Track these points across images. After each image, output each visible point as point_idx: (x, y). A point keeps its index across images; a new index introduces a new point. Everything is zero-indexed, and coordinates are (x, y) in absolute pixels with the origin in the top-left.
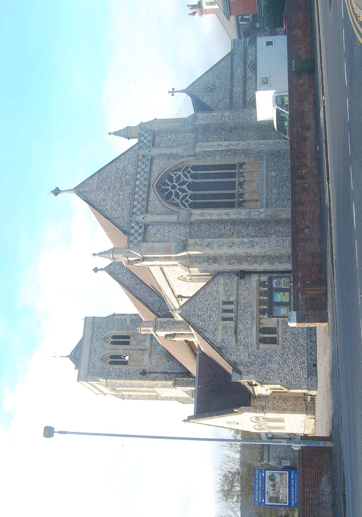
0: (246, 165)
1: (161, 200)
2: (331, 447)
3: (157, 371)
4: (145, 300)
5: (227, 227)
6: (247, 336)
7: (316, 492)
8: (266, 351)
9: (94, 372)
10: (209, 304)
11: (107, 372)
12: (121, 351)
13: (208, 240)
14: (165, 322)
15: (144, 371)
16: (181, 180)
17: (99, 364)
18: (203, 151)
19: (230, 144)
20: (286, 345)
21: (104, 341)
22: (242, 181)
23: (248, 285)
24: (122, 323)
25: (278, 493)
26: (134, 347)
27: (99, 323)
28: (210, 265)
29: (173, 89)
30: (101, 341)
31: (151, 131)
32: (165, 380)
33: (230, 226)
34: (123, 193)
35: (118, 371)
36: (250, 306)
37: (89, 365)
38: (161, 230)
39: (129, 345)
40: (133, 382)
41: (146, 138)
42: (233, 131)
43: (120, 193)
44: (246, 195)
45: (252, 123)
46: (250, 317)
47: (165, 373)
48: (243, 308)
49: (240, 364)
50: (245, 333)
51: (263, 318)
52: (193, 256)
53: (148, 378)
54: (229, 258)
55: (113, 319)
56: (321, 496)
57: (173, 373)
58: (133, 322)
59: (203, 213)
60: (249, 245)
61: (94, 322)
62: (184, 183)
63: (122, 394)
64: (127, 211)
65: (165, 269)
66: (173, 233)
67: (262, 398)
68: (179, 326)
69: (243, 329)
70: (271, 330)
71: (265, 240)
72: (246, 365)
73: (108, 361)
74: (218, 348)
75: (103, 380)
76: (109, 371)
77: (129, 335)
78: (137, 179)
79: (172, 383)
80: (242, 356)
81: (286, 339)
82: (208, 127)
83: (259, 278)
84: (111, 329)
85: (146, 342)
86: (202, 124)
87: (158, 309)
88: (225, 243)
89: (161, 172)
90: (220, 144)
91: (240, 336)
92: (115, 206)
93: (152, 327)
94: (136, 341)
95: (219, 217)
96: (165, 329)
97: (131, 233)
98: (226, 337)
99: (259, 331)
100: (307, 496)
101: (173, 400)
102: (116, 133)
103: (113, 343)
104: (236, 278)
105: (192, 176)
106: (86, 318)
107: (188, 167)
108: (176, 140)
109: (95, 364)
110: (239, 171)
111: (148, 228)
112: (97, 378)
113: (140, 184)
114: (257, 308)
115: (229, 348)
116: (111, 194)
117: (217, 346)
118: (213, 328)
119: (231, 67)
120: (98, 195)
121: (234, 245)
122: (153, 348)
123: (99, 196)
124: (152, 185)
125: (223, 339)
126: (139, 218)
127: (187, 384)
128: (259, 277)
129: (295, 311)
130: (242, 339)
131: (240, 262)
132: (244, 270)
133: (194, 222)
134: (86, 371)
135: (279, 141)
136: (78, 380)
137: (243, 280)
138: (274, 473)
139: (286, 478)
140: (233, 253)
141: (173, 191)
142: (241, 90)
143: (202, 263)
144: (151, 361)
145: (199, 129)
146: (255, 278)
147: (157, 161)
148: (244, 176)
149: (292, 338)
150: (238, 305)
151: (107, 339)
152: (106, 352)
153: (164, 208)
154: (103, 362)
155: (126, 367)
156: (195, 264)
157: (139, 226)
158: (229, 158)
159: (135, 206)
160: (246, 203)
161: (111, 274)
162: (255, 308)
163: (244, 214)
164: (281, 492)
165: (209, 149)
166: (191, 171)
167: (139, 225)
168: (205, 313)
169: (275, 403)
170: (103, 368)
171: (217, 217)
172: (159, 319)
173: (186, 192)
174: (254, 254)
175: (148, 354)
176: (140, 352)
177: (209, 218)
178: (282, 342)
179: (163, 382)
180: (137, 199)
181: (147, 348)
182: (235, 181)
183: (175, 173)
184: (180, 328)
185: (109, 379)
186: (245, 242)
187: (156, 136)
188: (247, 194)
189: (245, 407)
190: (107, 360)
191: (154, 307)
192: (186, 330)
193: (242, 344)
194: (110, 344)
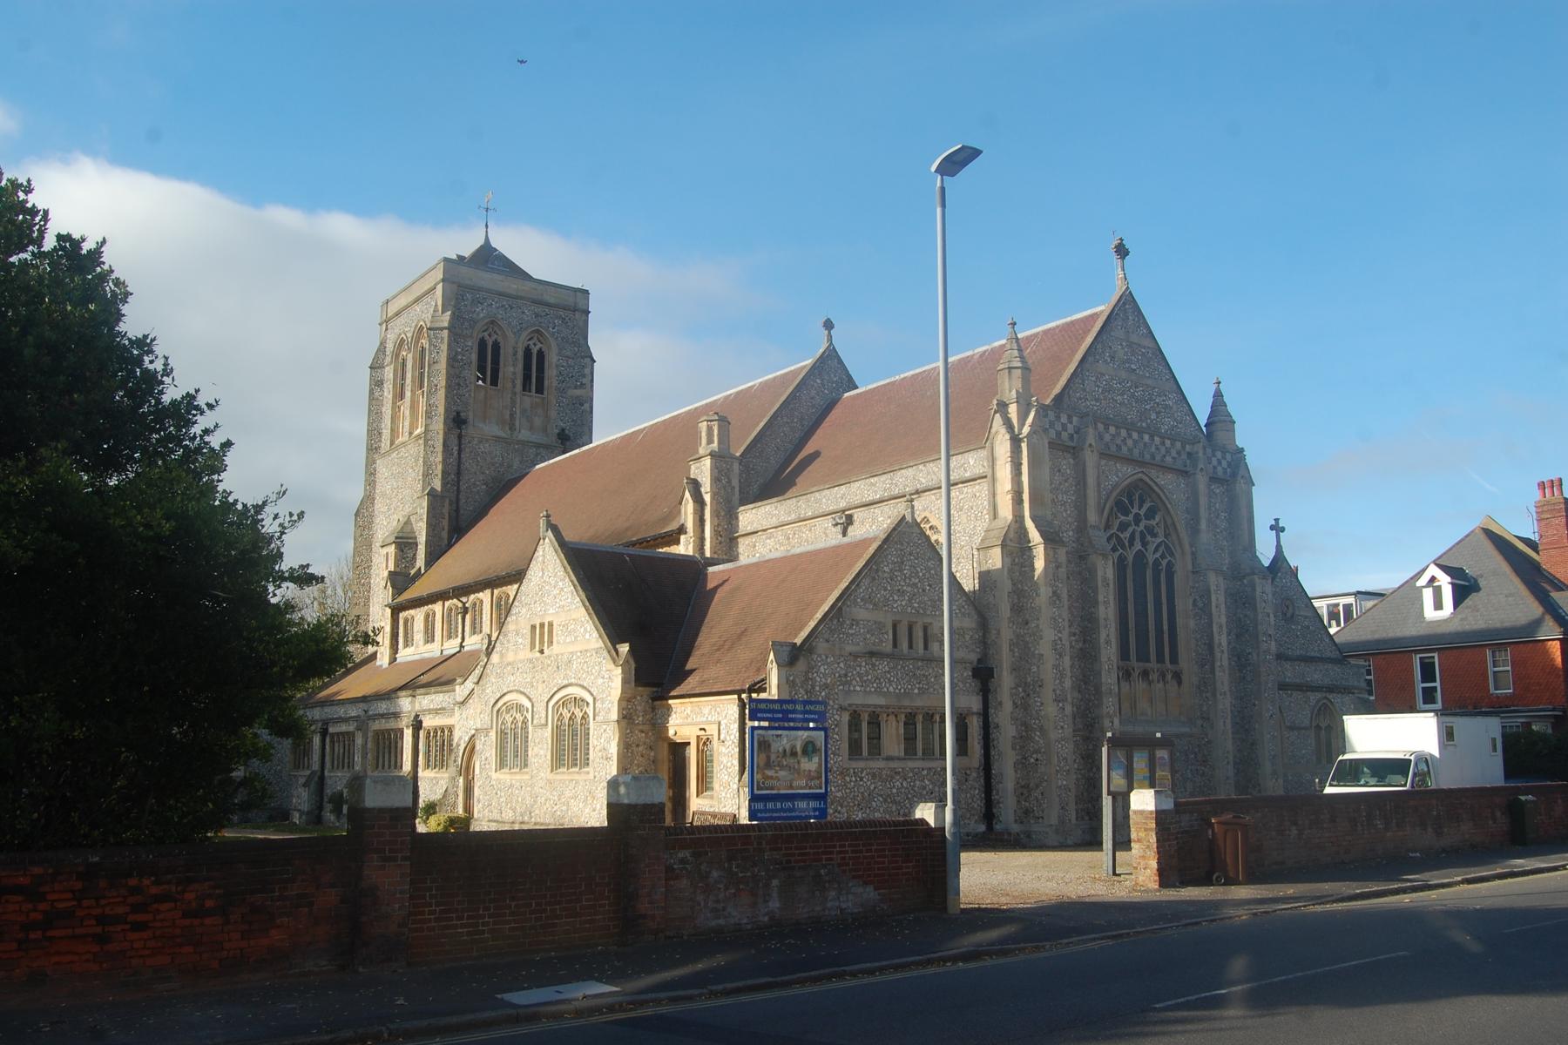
1: (1118, 491)
2: (945, 909)
4: (771, 435)
5: (1076, 641)
6: (865, 682)
7: (844, 871)
8: (837, 730)
10: (924, 591)
11: (464, 334)
12: (512, 369)
13: (1065, 595)
14: (729, 482)
15: (464, 422)
16: (1149, 538)
17: (482, 315)
18: (1209, 591)
19: (1223, 651)
20: (848, 779)
23: (961, 686)
24: (572, 376)
25: (779, 765)
26: (518, 401)
28: (1008, 596)
29: (1283, 529)
31: (1234, 475)
32: (443, 472)
33: (1078, 647)
34: (1126, 401)
36: (922, 692)
37: (480, 289)
38: (1066, 484)
40: (442, 393)
41: (1219, 462)
42: (1235, 659)
43: (1126, 397)
44: (1128, 683)
45: (1257, 703)
46: (902, 690)
47: (459, 473)
48: (918, 672)
49: (809, 663)
50: (870, 677)
51: (898, 722)
52: (1025, 557)
53: (449, 430)
54: (1021, 643)
55: (583, 357)
56: (836, 886)
57: (458, 491)
60: (1058, 692)
61: (577, 310)
62: (1144, 544)
63: (387, 365)
64: (1095, 408)
65: (982, 489)
66: (1062, 513)
67: (651, 716)
68: (723, 514)
69: (879, 671)
70: (875, 741)
71: (1069, 731)
72: (807, 679)
73: (487, 338)
74: (840, 608)
75: (445, 320)
77: (545, 392)
78: (1152, 437)
80: (825, 670)
81: (861, 780)
82: (1244, 604)
83: (973, 714)
86: (1254, 590)
87: (751, 466)
88: (1060, 635)
91: (864, 664)
92: (1104, 383)
93: (719, 448)
94: (531, 407)
95: (1102, 622)
96: (715, 480)
97: (1062, 415)
98: (862, 631)
99: (874, 712)
100: (834, 846)
101: (366, 490)
102: (1218, 395)
103: (528, 352)
104: (973, 657)
105: (1157, 563)
106: (587, 292)
107: (1172, 554)
108: (1218, 531)
111: (1069, 455)
113: (1145, 444)
114: (918, 708)
115: (841, 636)
116: (1123, 374)
117: (843, 609)
118: (879, 599)
119: (1323, 658)
120: (1121, 345)
121: (1058, 657)
123: (1119, 347)
124: (1144, 470)
125: (857, 624)
126: (1091, 439)
127: (435, 526)
128: (978, 714)
129: (1175, 805)
130: (858, 669)
131: (1014, 669)
132: (993, 677)
133: (1086, 564)
134: (468, 282)
135: (1232, 763)
136: (446, 260)
137: (970, 673)
138: (821, 755)
139: (810, 788)
140: (1037, 652)
141: (1131, 517)
142: (1287, 680)
143: (1012, 581)
144: (487, 440)
145: (1239, 583)
146: (975, 703)
149: (862, 793)
150: (925, 662)
151: (538, 339)
154: (487, 324)
156: (1008, 560)
157: (1073, 435)
159: (1107, 428)
161: (823, 359)
162: (918, 703)
163: (1109, 681)
164: (782, 773)
165: (1213, 604)
166: (1166, 561)
167: (1075, 435)
168: (908, 581)
169: (641, 749)
172: (736, 466)
173: (1130, 548)
174: (1036, 701)
175: (504, 435)
176: (507, 417)
177: (1101, 598)
178: (854, 769)
179: (440, 467)
180: (1118, 434)
182: (1148, 661)
184: (718, 517)
185: (449, 336)
186: (1064, 682)
187: (1223, 485)
188: (1128, 687)
189: (633, 672)
190: (490, 335)
191: (755, 456)
192: (715, 531)
193: (849, 670)
194: (525, 345)
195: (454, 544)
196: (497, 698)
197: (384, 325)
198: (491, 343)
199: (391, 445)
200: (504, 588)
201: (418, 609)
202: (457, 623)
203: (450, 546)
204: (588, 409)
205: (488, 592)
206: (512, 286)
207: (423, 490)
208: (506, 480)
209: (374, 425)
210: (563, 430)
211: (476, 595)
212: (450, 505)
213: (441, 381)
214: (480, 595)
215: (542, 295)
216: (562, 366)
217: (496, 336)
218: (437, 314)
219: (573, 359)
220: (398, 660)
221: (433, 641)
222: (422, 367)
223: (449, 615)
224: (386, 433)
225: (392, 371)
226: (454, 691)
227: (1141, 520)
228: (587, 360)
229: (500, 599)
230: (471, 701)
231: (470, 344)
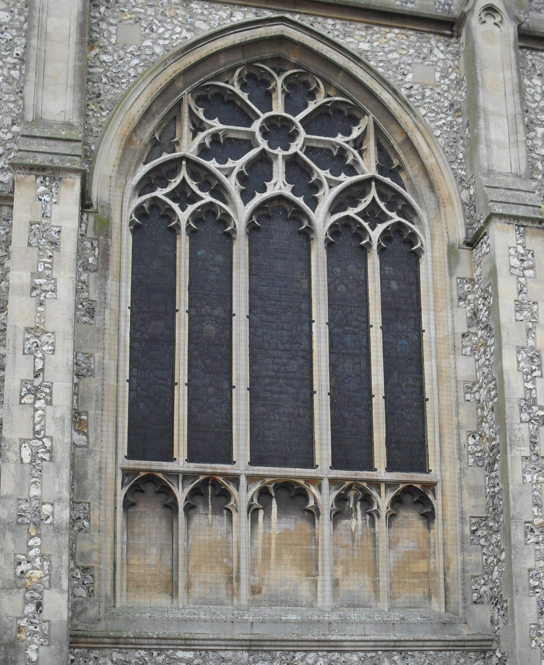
0: (425, 530)
16: (323, 174)
22: (312, 503)
59: (53, 243)
89: (368, 68)
90: (539, 366)
110: (376, 484)
141: (256, 127)
147: (442, 56)
148: (349, 517)
153: (135, 67)
158: (459, 427)
160: (164, 524)
163: (35, 491)
171: (22, 324)
173: (246, 196)
183: (371, 145)
227: (296, 133)
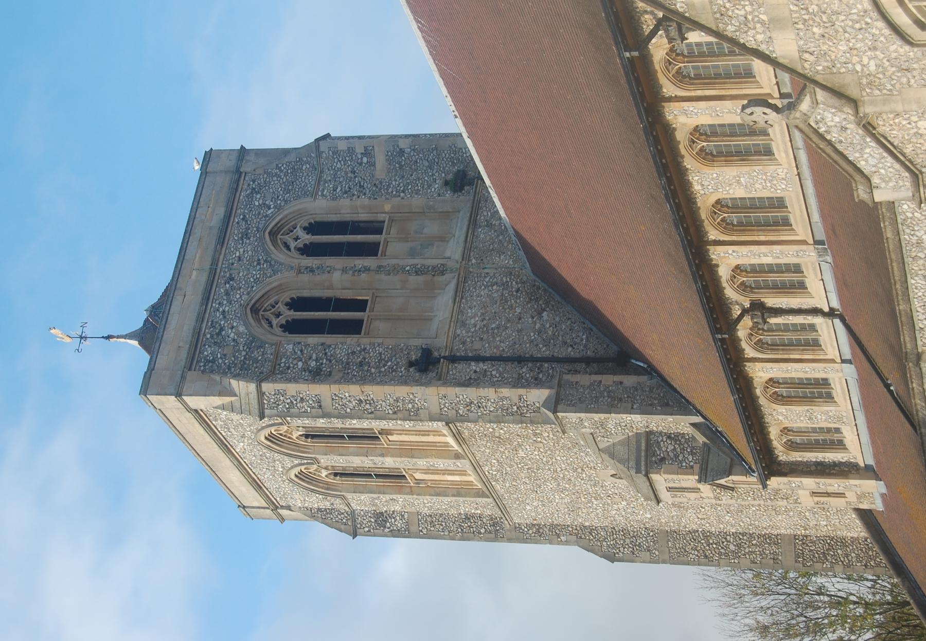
3: (483, 354)
9: (213, 361)
12: (337, 275)
17: (242, 329)
21: (274, 242)
24: (353, 172)
26: (393, 262)
27: (257, 172)
30: (262, 239)
32: (515, 386)
35: (314, 357)
37: (197, 333)
39: (377, 256)
40: (375, 392)
47: (520, 360)
53: (440, 379)
55: (319, 154)
57: (552, 360)
58: (401, 167)
63: (348, 505)
73: (282, 320)
75: (244, 388)
76: (277, 355)
77: (381, 217)
79: (543, 398)
84: (305, 194)
85: (451, 243)
94: (406, 240)
101: (567, 543)
103: (308, 250)
109: (222, 329)
112: (225, 381)
122: (474, 261)
127: (613, 399)
134: (184, 355)
152: (275, 281)
154: (258, 321)
155: (351, 340)
170: (253, 343)
175: (452, 285)
176: (420, 279)
179: (505, 392)
181: (450, 264)
185: (275, 381)
190: (278, 315)
195: (645, 360)
196: (887, 31)
197: (281, 511)
198: (292, 313)
199: (483, 495)
200: (703, 216)
201: (768, 419)
202: (786, 328)
203: (651, 370)
204: (410, 139)
205: (717, 254)
206: (196, 279)
207: (546, 422)
208: (533, 277)
209: (454, 528)
210: (446, 183)
211: (725, 285)
212: (576, 372)
213: (352, 392)
214: (724, 272)
215: (211, 228)
216: (335, 190)
217: (280, 304)
218: (237, 405)
219: (322, 172)
220: (871, 461)
221: (825, 382)
222: (337, 436)
223: (773, 347)
224: (467, 506)
225: (356, 496)
226: (891, 205)
228: (324, 146)
229: (726, 226)
230: (908, 150)
231: (291, 346)
